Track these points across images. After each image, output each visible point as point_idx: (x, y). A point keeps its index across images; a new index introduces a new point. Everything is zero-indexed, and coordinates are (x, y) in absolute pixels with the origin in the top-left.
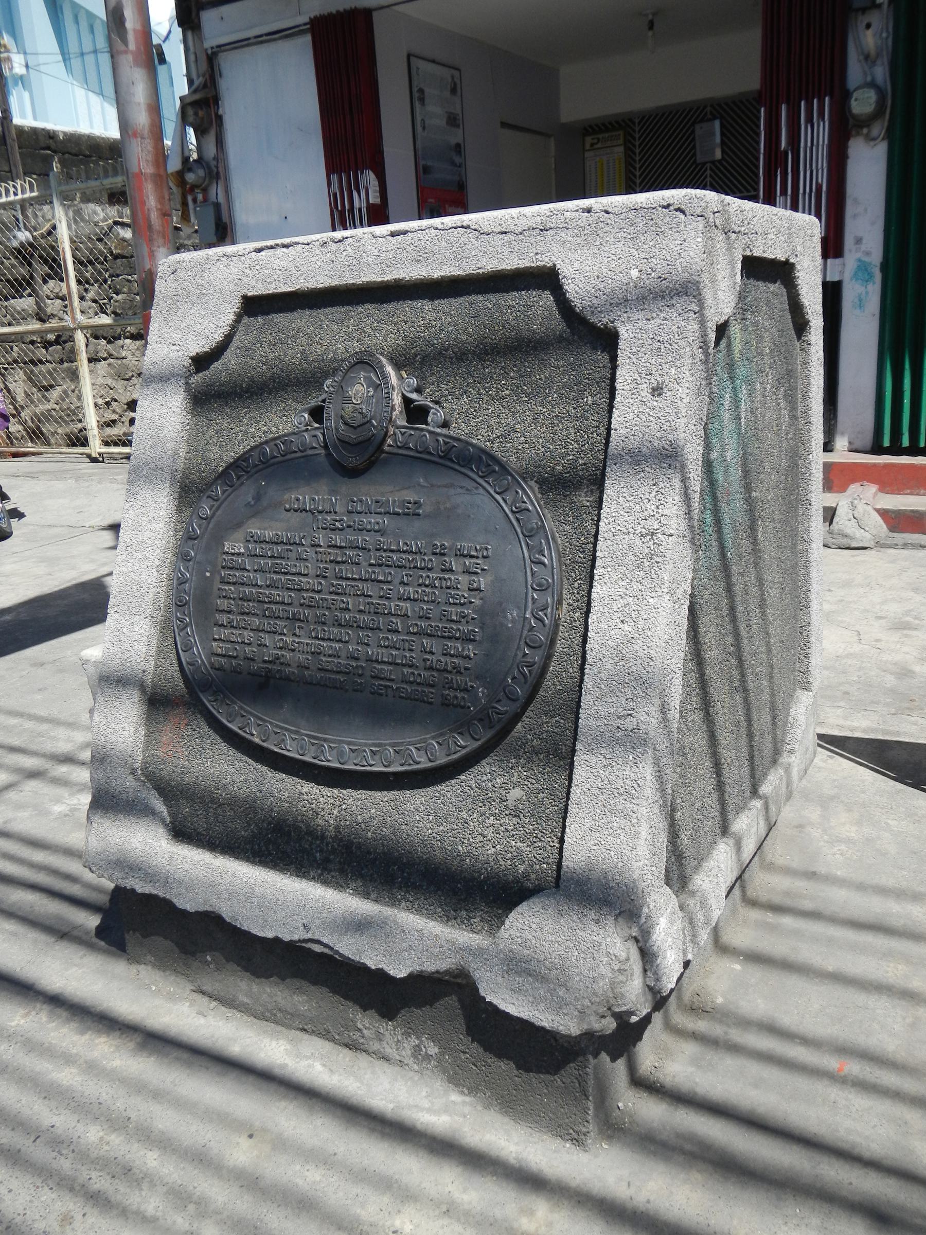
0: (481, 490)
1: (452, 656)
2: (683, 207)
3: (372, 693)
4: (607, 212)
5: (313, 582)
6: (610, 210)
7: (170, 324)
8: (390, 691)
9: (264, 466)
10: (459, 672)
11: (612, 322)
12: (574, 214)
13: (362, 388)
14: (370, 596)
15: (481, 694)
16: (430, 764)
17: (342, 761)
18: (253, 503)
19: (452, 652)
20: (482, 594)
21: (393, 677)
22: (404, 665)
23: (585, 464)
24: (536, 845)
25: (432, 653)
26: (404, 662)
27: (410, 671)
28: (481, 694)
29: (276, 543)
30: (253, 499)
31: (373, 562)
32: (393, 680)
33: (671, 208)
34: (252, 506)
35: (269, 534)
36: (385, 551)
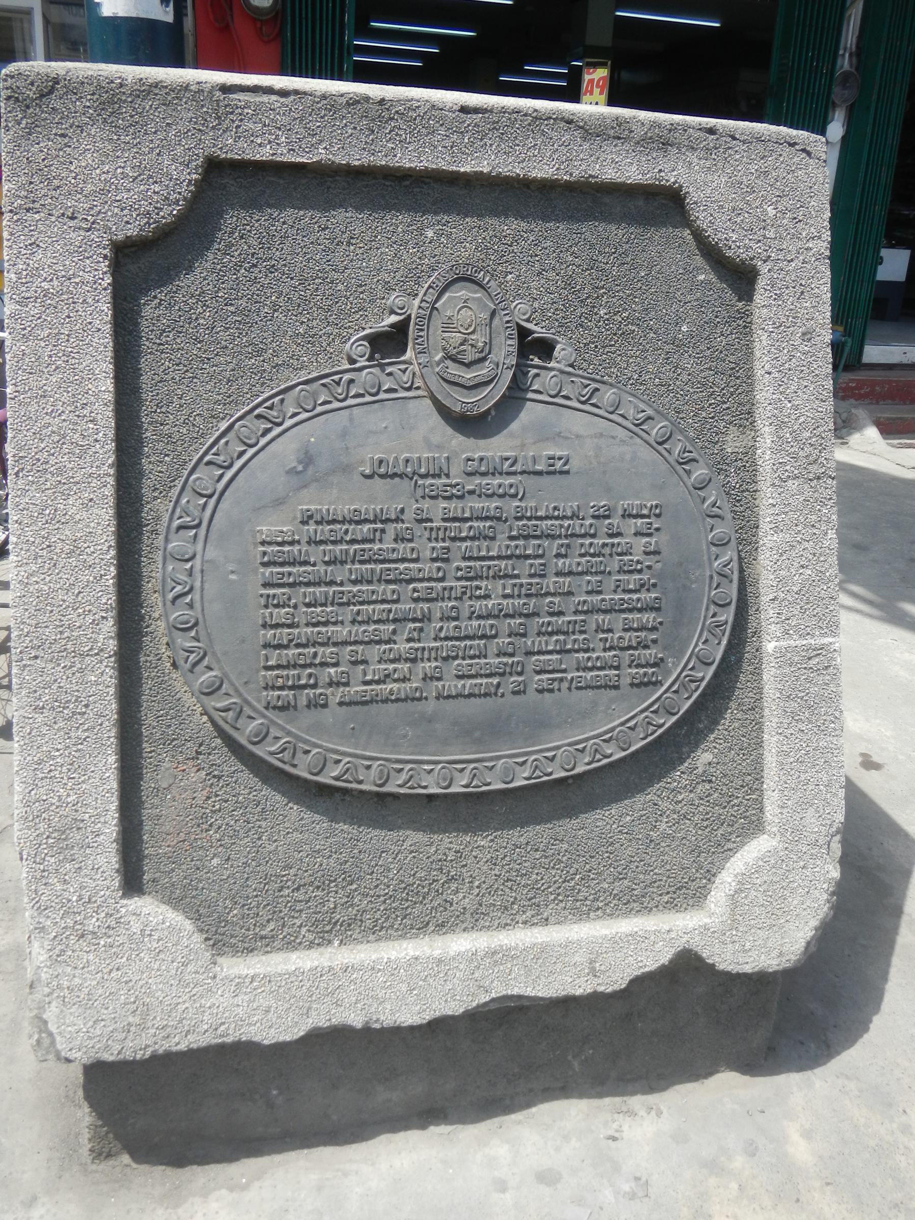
0: (639, 441)
1: (636, 630)
2: (808, 149)
3: (540, 691)
4: (734, 138)
5: (429, 568)
6: (737, 136)
7: (56, 182)
8: (565, 685)
9: (307, 415)
10: (646, 647)
11: (752, 259)
12: (699, 133)
13: (470, 313)
14: (517, 576)
15: (670, 665)
16: (623, 754)
17: (508, 780)
18: (300, 468)
19: (635, 625)
20: (657, 558)
21: (563, 666)
22: (577, 651)
23: (728, 408)
24: (732, 803)
25: (610, 631)
26: (576, 647)
27: (586, 655)
28: (670, 665)
29: (358, 523)
30: (300, 462)
31: (514, 533)
32: (564, 671)
33: (797, 147)
34: (301, 472)
35: (345, 509)
36: (529, 519)
